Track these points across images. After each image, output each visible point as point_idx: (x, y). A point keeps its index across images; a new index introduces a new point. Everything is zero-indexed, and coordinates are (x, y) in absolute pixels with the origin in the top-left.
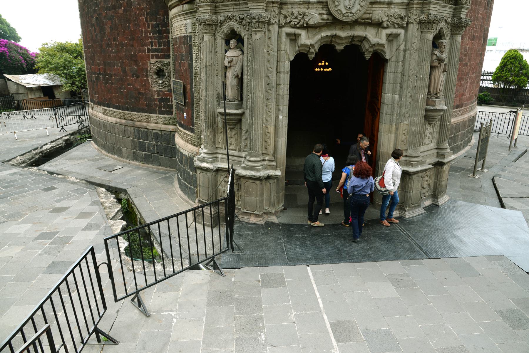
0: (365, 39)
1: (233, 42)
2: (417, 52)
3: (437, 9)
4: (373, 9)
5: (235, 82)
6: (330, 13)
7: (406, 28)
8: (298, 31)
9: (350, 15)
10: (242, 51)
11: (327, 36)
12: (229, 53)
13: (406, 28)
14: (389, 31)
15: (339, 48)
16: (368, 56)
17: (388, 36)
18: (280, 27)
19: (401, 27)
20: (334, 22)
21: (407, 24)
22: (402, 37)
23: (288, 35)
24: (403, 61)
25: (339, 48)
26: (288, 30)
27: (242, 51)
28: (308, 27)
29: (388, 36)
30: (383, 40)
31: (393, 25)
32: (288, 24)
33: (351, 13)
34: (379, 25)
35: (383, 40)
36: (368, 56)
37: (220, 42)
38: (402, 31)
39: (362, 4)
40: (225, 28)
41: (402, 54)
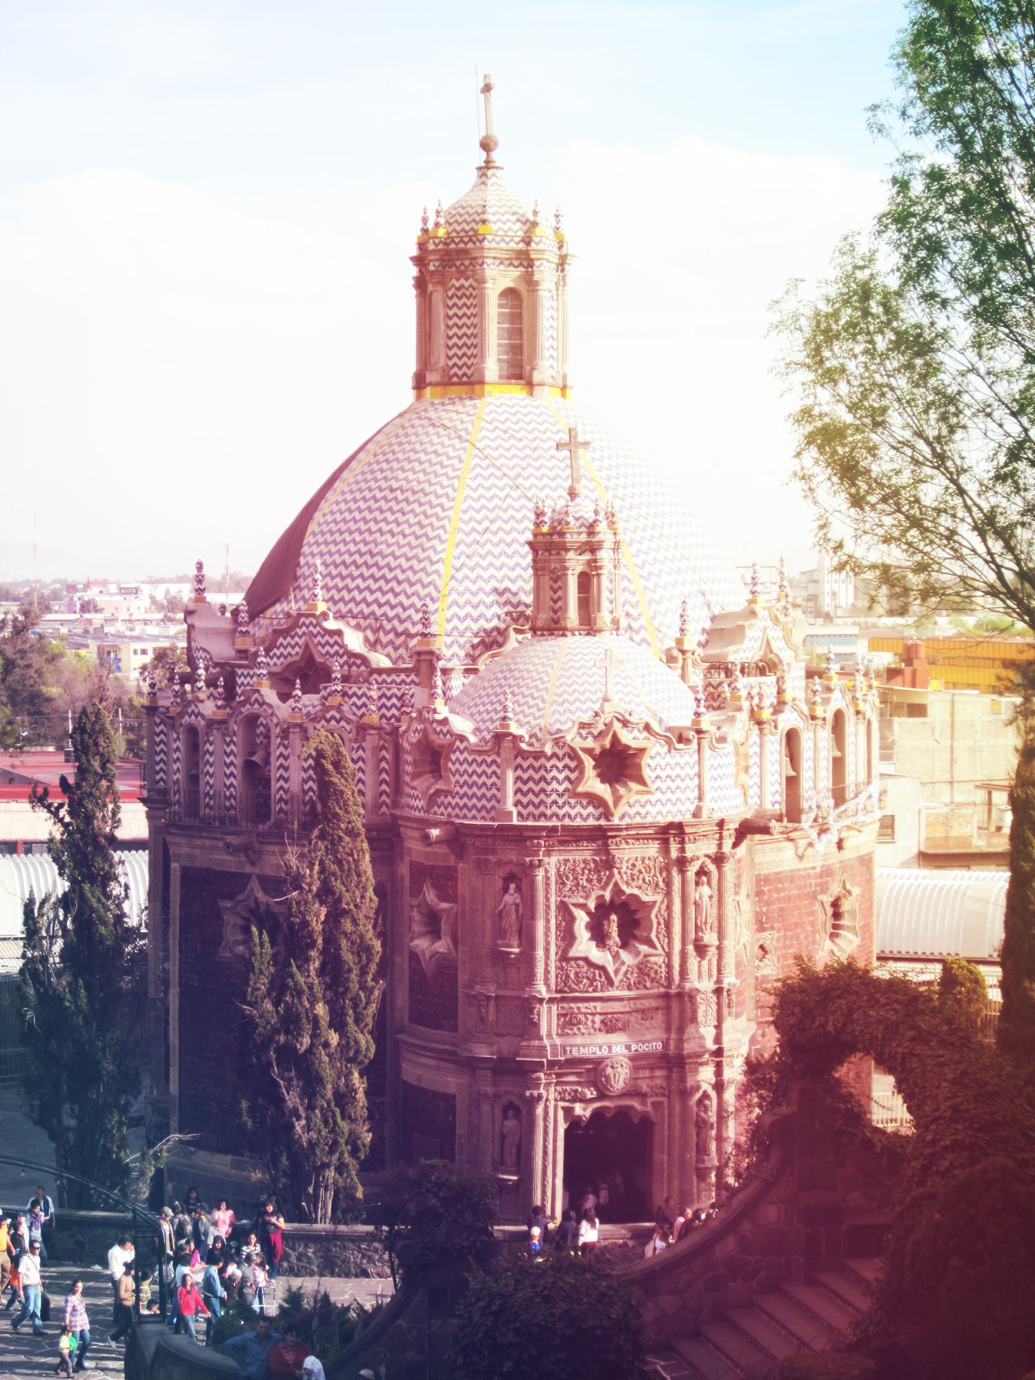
0: (632, 1107)
1: (511, 1113)
5: (514, 1150)
10: (520, 1121)
12: (507, 1123)
13: (669, 1097)
15: (608, 1115)
16: (636, 1121)
17: (653, 1104)
18: (556, 1100)
19: (663, 1095)
22: (666, 1104)
23: (563, 1108)
24: (669, 1125)
25: (608, 1115)
26: (561, 1104)
27: (520, 1121)
29: (653, 1104)
30: (649, 1108)
31: (657, 1095)
32: (563, 1099)
35: (649, 1108)
36: (636, 1121)
37: (498, 1112)
38: (665, 1100)
40: (505, 1100)
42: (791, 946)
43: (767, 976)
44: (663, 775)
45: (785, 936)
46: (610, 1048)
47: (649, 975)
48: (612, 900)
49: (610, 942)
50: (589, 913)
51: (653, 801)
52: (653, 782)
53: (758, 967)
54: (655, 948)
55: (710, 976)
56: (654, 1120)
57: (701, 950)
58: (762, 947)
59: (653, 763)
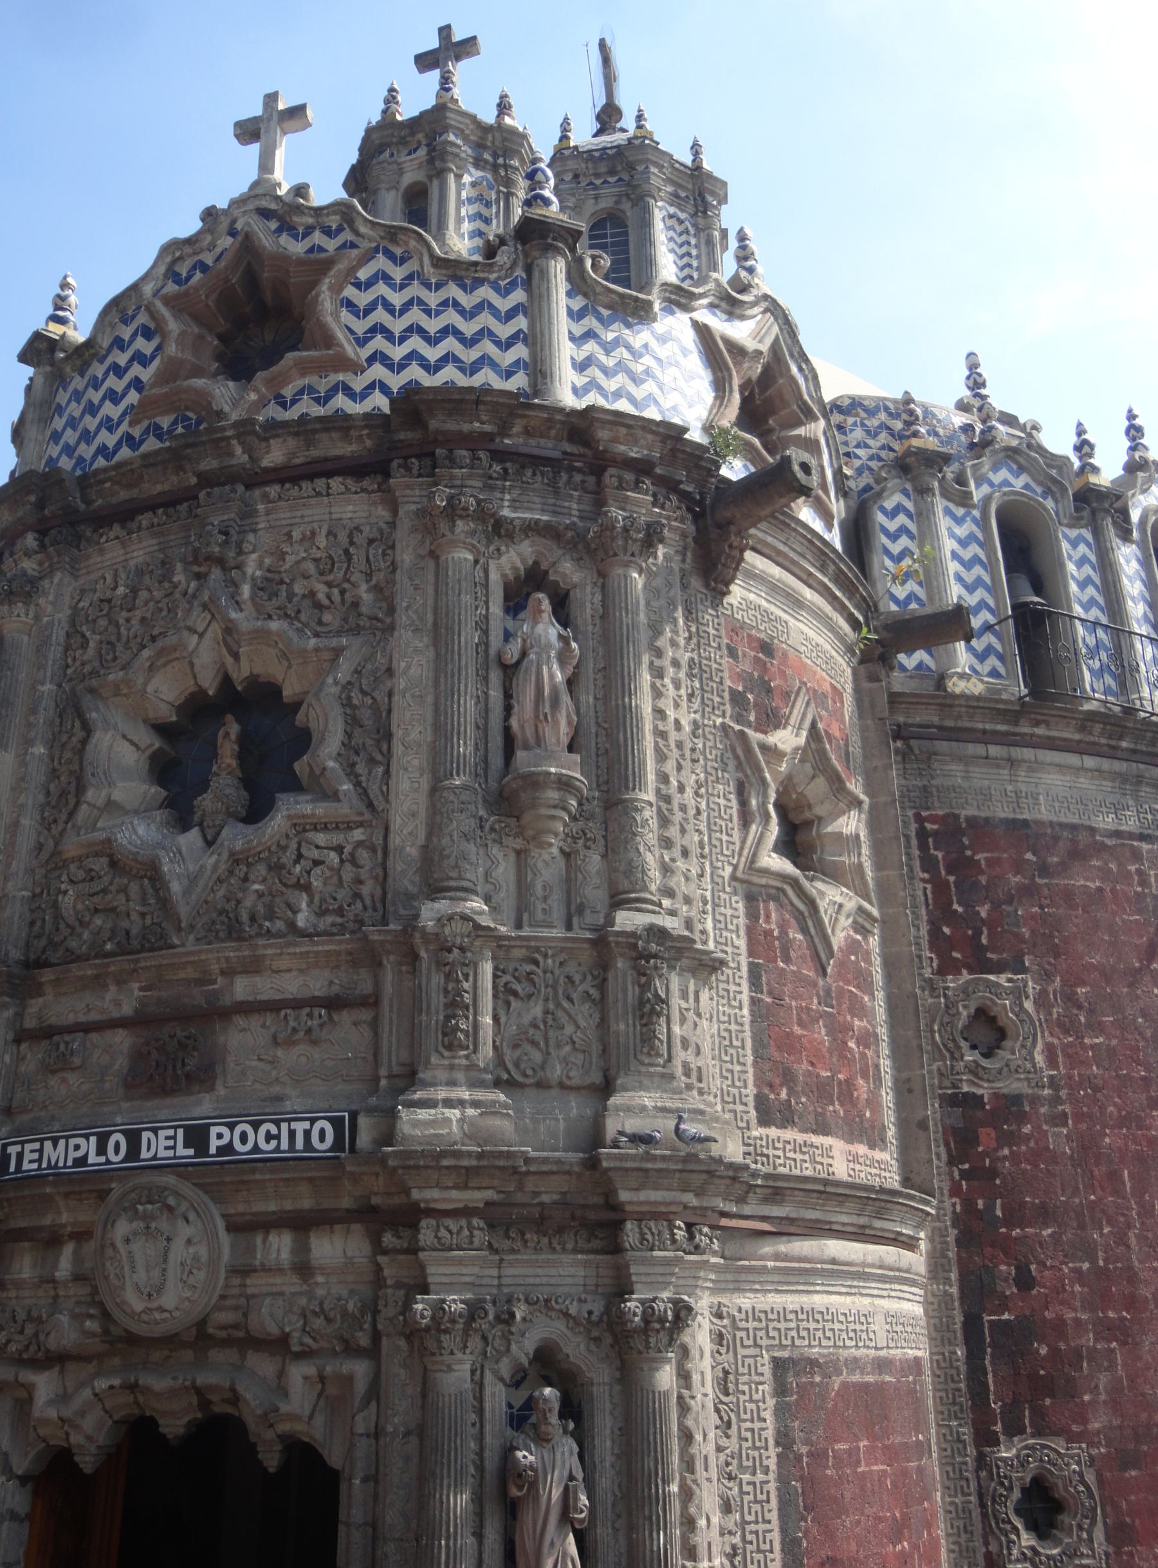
2: (414, 1440)
3: (468, 1279)
4: (250, 1291)
6: (106, 1315)
7: (373, 1352)
8: (27, 1376)
9: (158, 1316)
11: (112, 1387)
13: (373, 1352)
14: (309, 1369)
16: (271, 1460)
20: (124, 1343)
21: (376, 1336)
28: (58, 1360)
33: (162, 1310)
34: (279, 1345)
36: (271, 1460)
39: (191, 1280)
41: (363, 1447)
42: (1097, 1027)
43: (1017, 1099)
44: (397, 326)
45: (1070, 999)
46: (133, 1139)
47: (307, 888)
48: (226, 681)
49: (206, 802)
50: (161, 729)
51: (358, 383)
52: (362, 342)
53: (975, 1070)
54: (335, 796)
55: (573, 911)
56: (334, 1458)
57: (509, 800)
58: (984, 1016)
59: (363, 299)
